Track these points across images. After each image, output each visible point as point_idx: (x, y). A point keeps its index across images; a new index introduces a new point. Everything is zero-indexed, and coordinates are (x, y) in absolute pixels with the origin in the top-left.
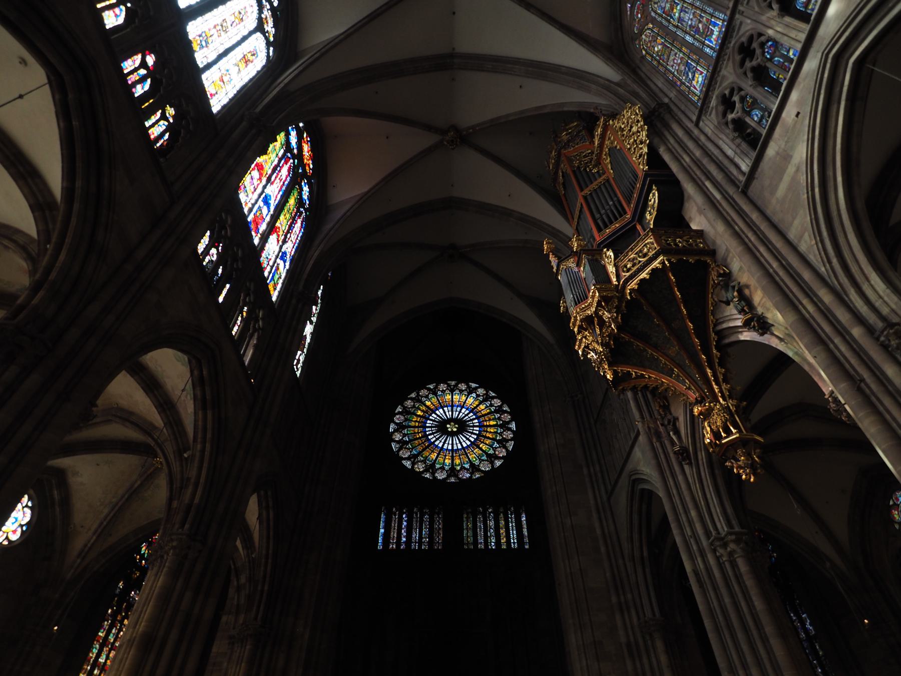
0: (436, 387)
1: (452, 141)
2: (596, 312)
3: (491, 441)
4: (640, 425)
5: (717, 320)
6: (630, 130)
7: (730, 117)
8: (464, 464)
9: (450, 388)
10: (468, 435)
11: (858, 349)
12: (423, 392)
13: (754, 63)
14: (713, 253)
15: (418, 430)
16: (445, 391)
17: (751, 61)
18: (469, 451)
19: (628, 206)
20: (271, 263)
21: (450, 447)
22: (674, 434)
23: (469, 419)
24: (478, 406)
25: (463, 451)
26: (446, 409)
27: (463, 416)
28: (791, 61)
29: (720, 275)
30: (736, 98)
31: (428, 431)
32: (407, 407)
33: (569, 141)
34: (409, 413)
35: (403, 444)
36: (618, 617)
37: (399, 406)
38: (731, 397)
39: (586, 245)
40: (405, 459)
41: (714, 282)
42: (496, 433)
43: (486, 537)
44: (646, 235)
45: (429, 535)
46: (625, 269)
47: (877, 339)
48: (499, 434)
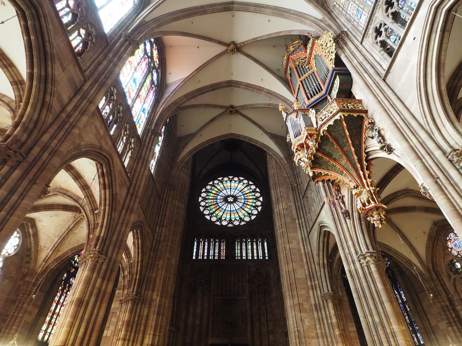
0: (222, 179)
1: (232, 50)
2: (305, 142)
4: (325, 199)
5: (367, 146)
6: (326, 46)
7: (379, 39)
11: (437, 162)
12: (216, 182)
13: (393, 10)
14: (366, 112)
17: (392, 8)
19: (324, 86)
20: (138, 114)
21: (229, 209)
22: (343, 204)
24: (244, 189)
28: (413, 9)
29: (369, 123)
30: (382, 29)
33: (294, 51)
34: (209, 192)
35: (205, 207)
37: (204, 189)
38: (371, 185)
39: (301, 107)
40: (206, 215)
41: (366, 127)
42: (253, 202)
44: (333, 102)
45: (218, 252)
46: (321, 120)
47: (447, 157)
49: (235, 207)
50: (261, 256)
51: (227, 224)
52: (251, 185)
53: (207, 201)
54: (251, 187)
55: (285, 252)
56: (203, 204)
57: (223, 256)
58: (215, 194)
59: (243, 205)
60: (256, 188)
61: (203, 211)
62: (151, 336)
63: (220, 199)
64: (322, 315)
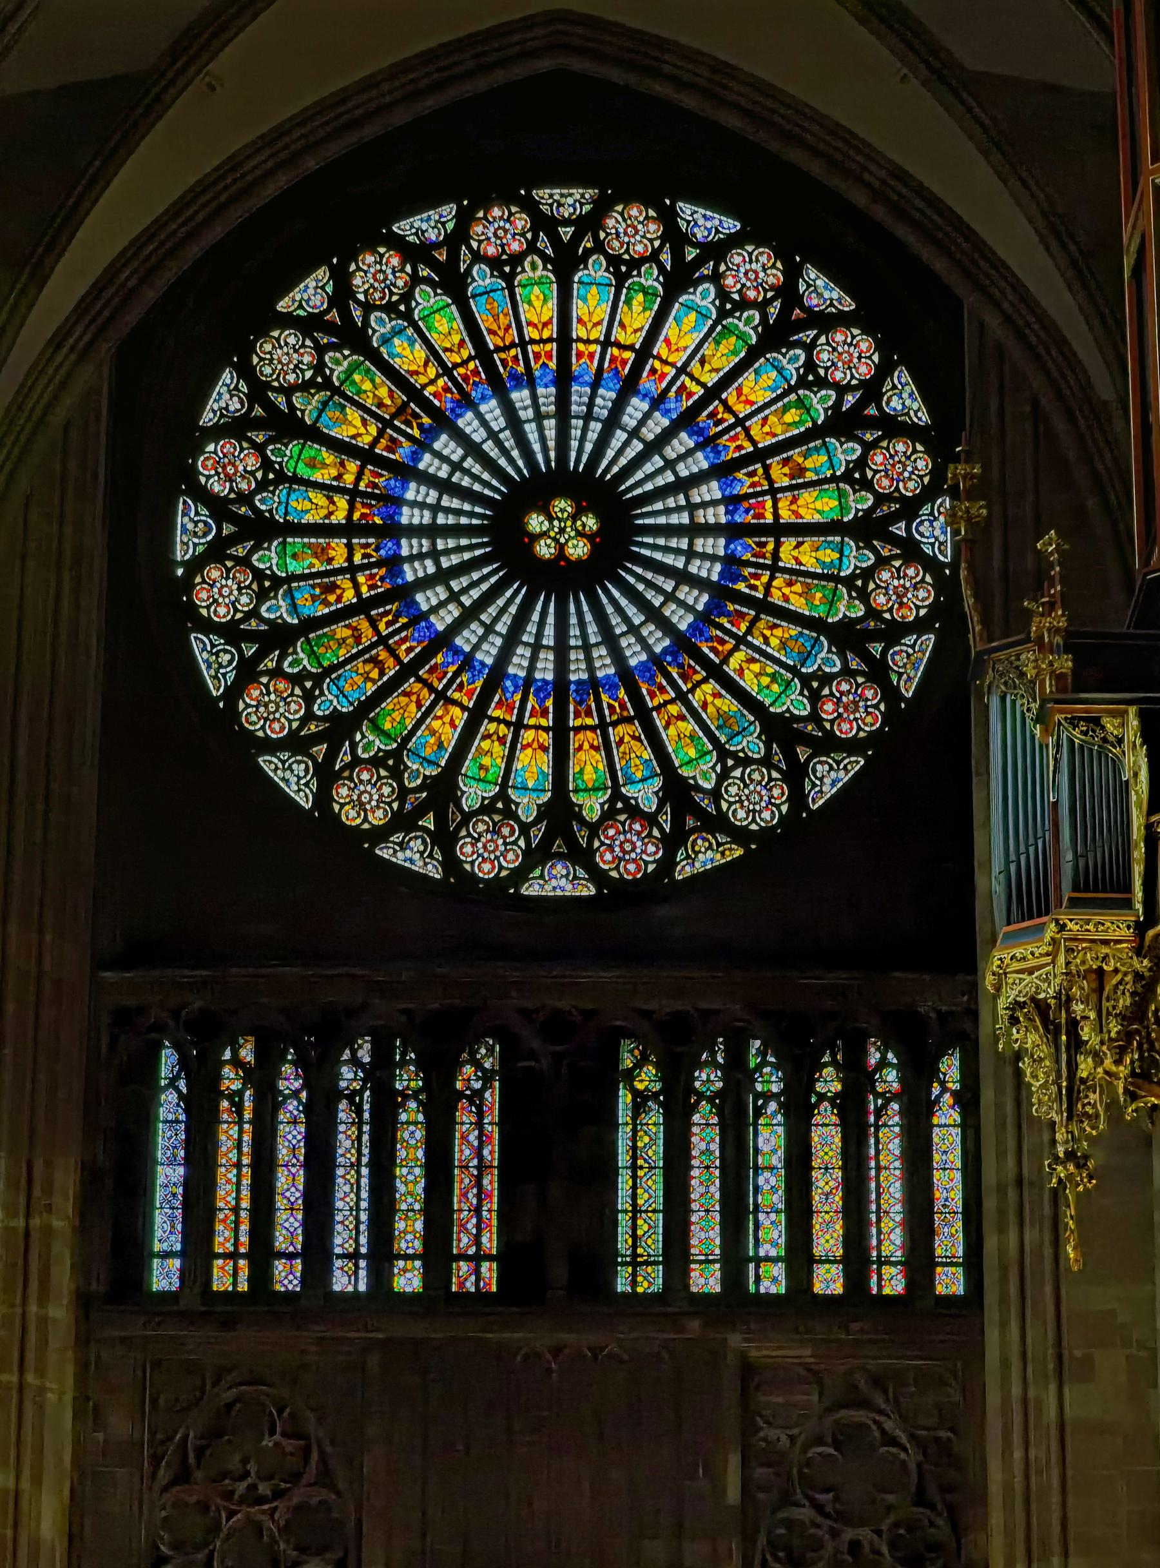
0: (459, 237)
2: (1064, 1000)
3: (794, 631)
9: (555, 239)
10: (659, 590)
15: (350, 547)
16: (516, 260)
18: (660, 699)
21: (546, 671)
23: (669, 477)
25: (622, 694)
26: (520, 397)
27: (630, 453)
31: (411, 558)
32: (267, 386)
37: (227, 376)
40: (270, 746)
45: (427, 1239)
48: (849, 582)
49: (610, 639)
50: (882, 1262)
51: (512, 860)
52: (826, 322)
53: (268, 559)
55: (1018, 1454)
57: (477, 1259)
58: (366, 456)
59: (705, 619)
60: (884, 371)
61: (234, 693)
63: (432, 531)
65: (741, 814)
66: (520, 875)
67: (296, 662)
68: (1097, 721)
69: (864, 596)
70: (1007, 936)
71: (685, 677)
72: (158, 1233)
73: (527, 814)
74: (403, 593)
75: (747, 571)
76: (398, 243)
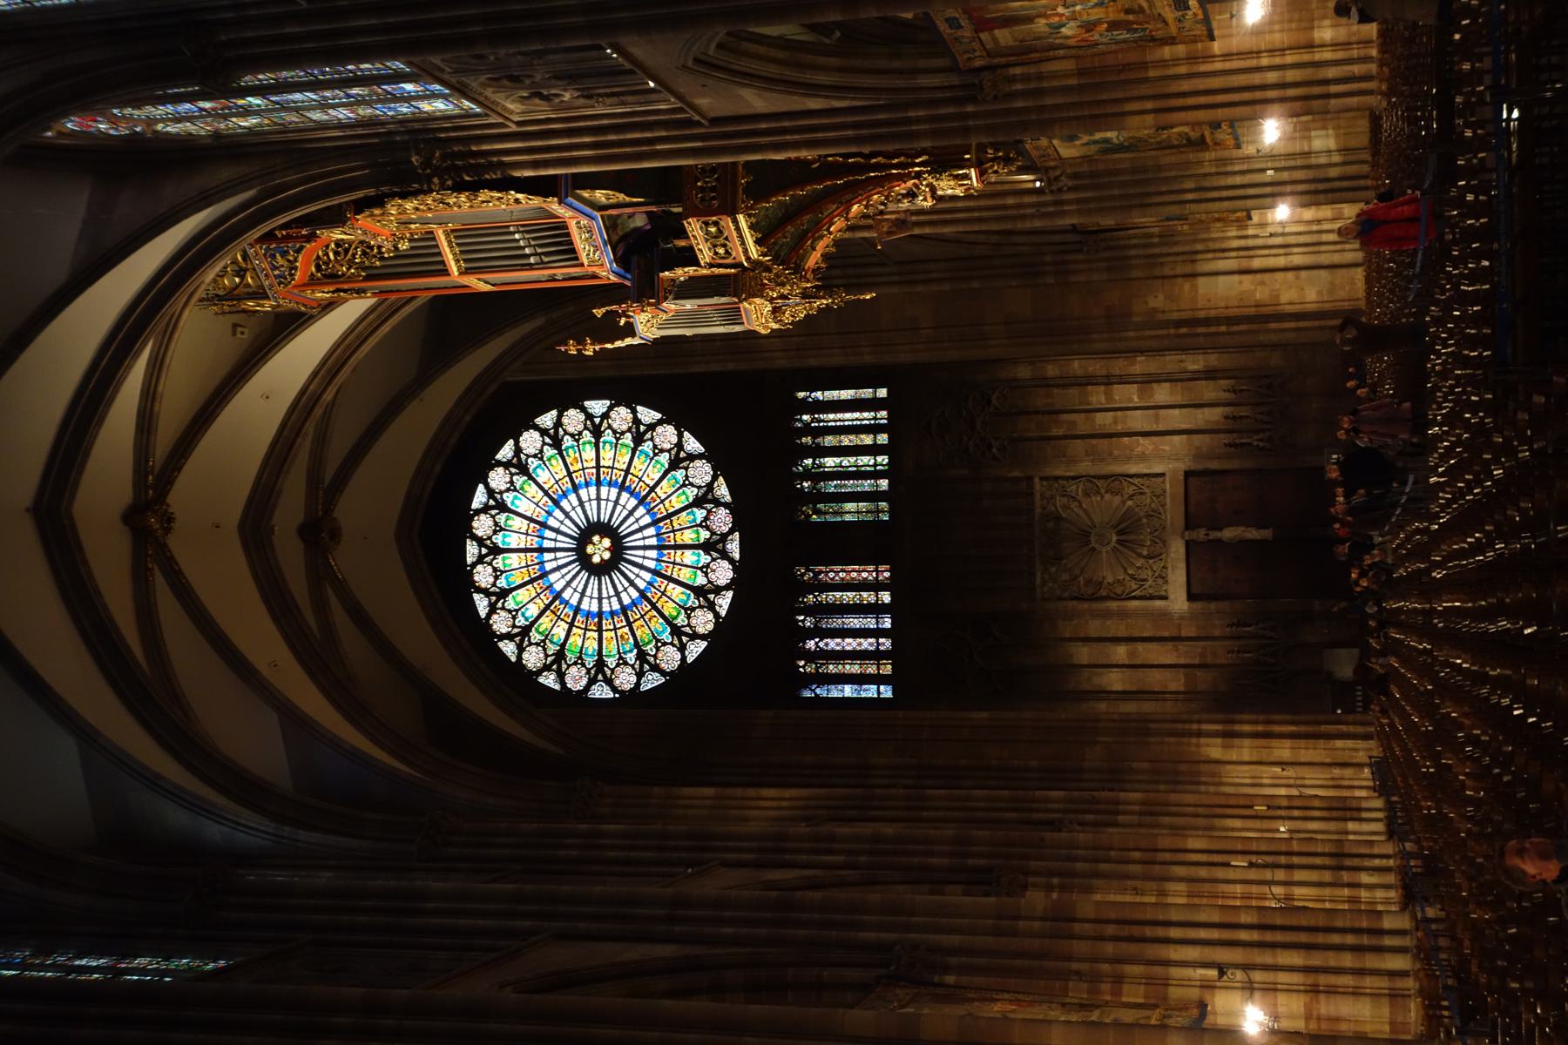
0: (486, 592)
2: (771, 300)
3: (636, 459)
8: (694, 520)
12: (500, 623)
15: (606, 630)
16: (495, 570)
18: (663, 510)
21: (653, 554)
25: (661, 524)
26: (548, 567)
34: (560, 655)
36: (1074, 279)
37: (541, 680)
40: (684, 658)
43: (860, 475)
48: (618, 439)
49: (641, 529)
51: (726, 564)
52: (518, 450)
54: (532, 451)
56: (626, 679)
58: (571, 625)
59: (632, 493)
60: (536, 428)
61: (663, 673)
62: (1202, 740)
64: (1136, 257)
65: (706, 478)
66: (731, 561)
67: (651, 649)
68: (665, 289)
69: (623, 433)
70: (749, 324)
71: (655, 501)
72: (870, 695)
73: (709, 559)
74: (624, 610)
75: (614, 478)
76: (489, 616)
